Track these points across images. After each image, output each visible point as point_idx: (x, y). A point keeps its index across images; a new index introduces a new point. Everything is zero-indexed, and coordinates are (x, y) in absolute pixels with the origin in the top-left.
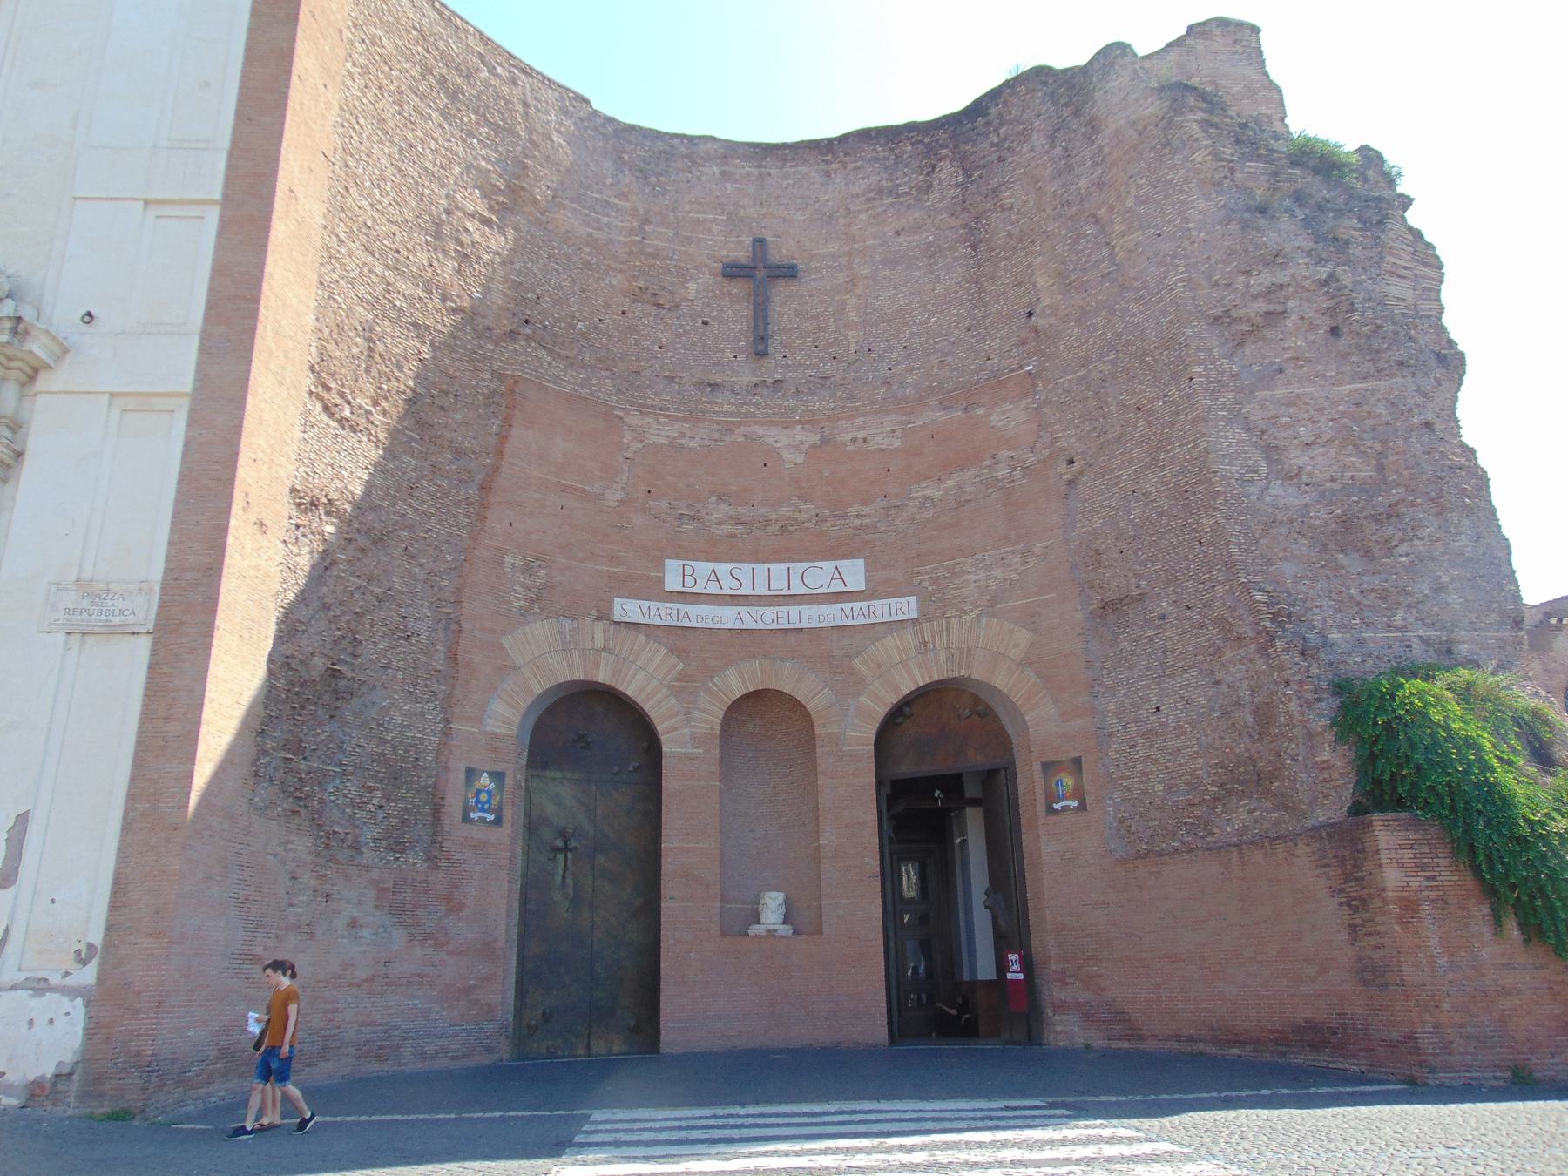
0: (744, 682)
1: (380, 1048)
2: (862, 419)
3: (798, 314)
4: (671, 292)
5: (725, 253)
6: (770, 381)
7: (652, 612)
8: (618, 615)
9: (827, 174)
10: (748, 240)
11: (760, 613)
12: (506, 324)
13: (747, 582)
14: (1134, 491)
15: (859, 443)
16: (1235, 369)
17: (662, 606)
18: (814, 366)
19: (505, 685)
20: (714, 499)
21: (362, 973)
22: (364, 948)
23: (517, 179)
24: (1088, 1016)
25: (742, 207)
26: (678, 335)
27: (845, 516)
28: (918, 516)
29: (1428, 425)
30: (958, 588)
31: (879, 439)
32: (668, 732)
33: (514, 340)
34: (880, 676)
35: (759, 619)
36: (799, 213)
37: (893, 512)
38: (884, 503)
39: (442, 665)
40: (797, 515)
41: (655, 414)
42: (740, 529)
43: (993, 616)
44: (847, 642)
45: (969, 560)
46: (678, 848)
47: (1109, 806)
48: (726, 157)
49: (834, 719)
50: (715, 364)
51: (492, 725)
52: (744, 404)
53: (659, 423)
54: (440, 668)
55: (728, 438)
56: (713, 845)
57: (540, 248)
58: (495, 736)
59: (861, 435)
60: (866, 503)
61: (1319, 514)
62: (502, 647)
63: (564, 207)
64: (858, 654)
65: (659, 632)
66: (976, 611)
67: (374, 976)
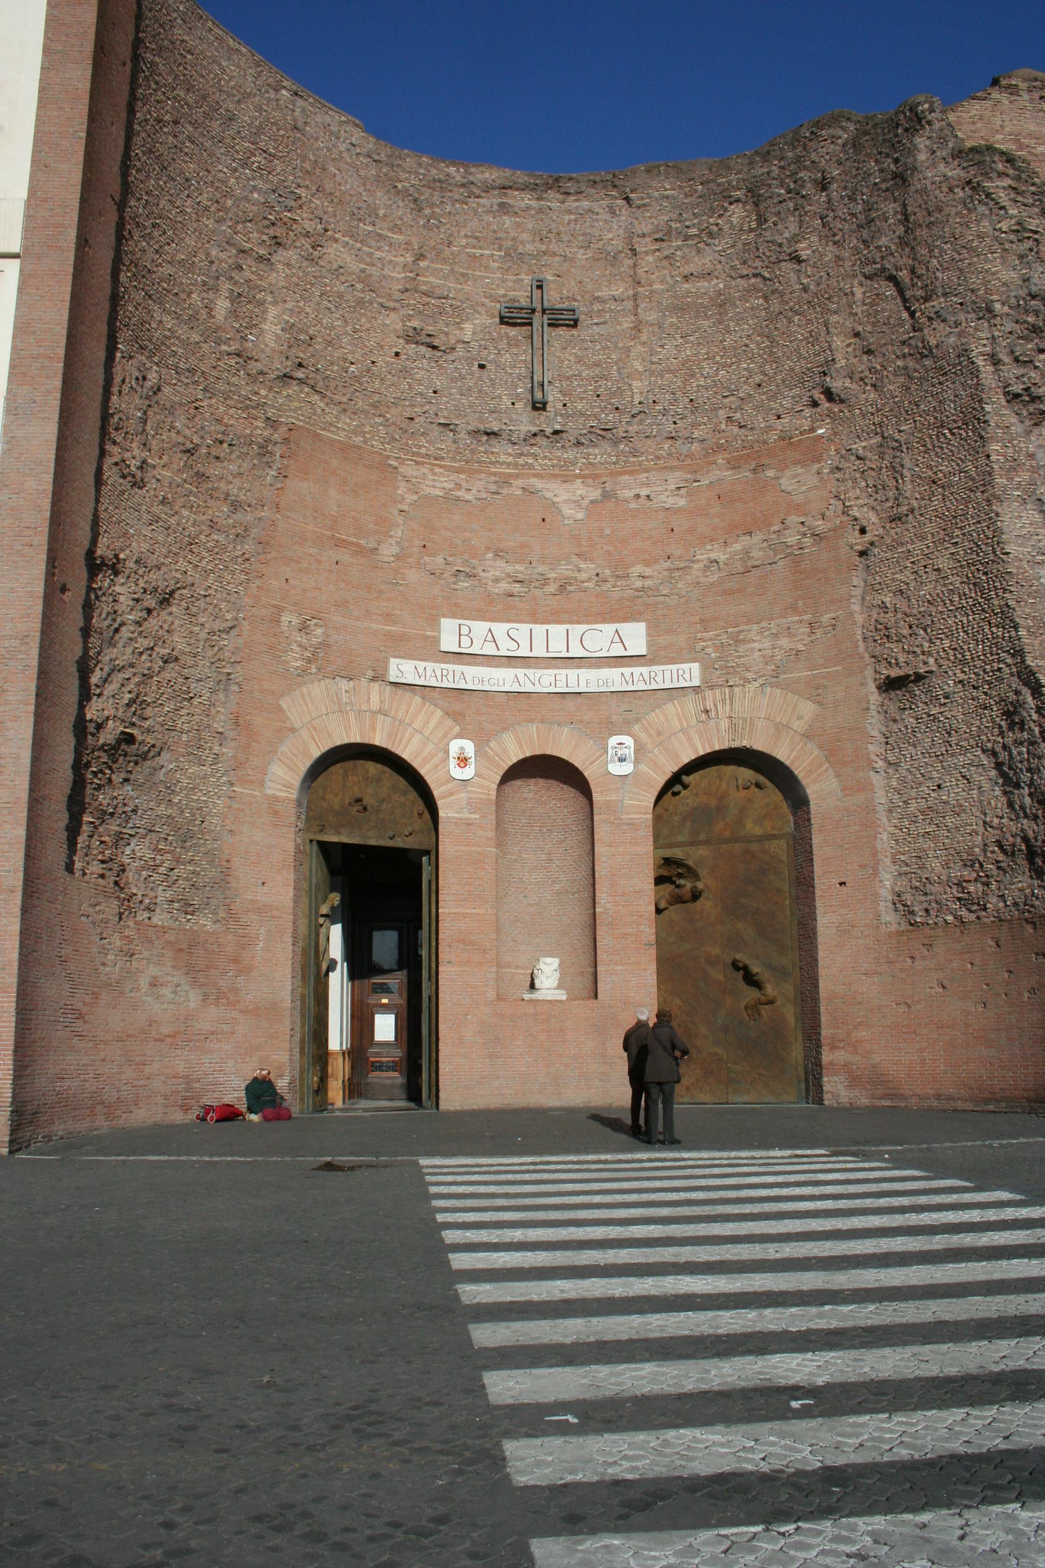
0: (521, 747)
1: (186, 1098)
2: (646, 475)
3: (579, 360)
4: (447, 334)
5: (502, 292)
6: (549, 431)
7: (428, 674)
8: (393, 676)
9: (612, 212)
10: (527, 279)
11: (538, 676)
12: (279, 366)
13: (525, 644)
14: (925, 567)
15: (642, 501)
16: (1031, 449)
17: (438, 667)
18: (596, 416)
19: (284, 748)
20: (490, 555)
21: (166, 1030)
22: (165, 1006)
23: (289, 211)
24: (854, 1081)
25: (521, 243)
26: (453, 380)
27: (627, 576)
28: (703, 580)
30: (741, 656)
31: (663, 498)
32: (444, 797)
33: (286, 385)
34: (660, 744)
35: (537, 683)
36: (582, 251)
37: (677, 574)
38: (668, 564)
39: (223, 727)
40: (577, 575)
41: (430, 464)
42: (517, 588)
43: (777, 685)
44: (627, 708)
45: (755, 627)
46: (456, 913)
47: (887, 880)
48: (504, 188)
49: (612, 786)
50: (492, 412)
51: (272, 789)
52: (521, 454)
53: (434, 474)
54: (220, 730)
55: (504, 491)
56: (490, 911)
57: (312, 285)
58: (275, 799)
59: (644, 492)
60: (648, 563)
62: (280, 709)
63: (336, 240)
64: (637, 720)
65: (435, 694)
66: (761, 681)
67: (175, 1033)
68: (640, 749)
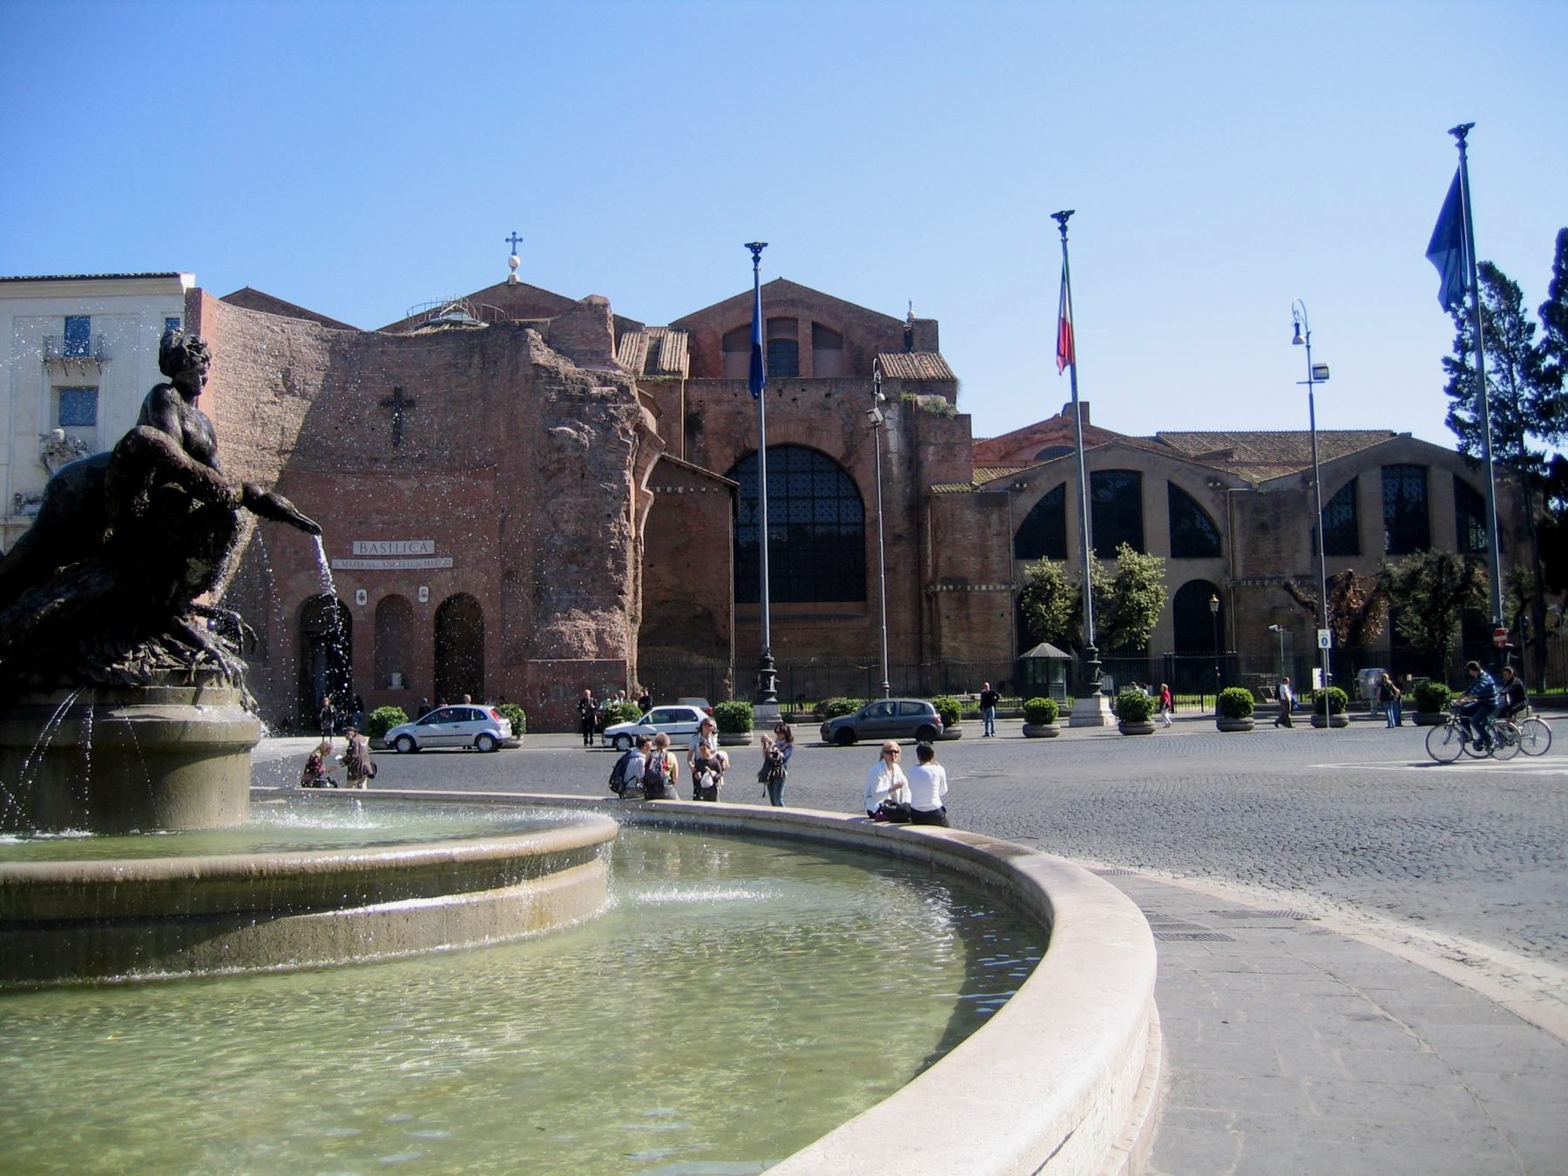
9: (429, 351)
17: (352, 562)
29: (609, 516)
61: (566, 548)
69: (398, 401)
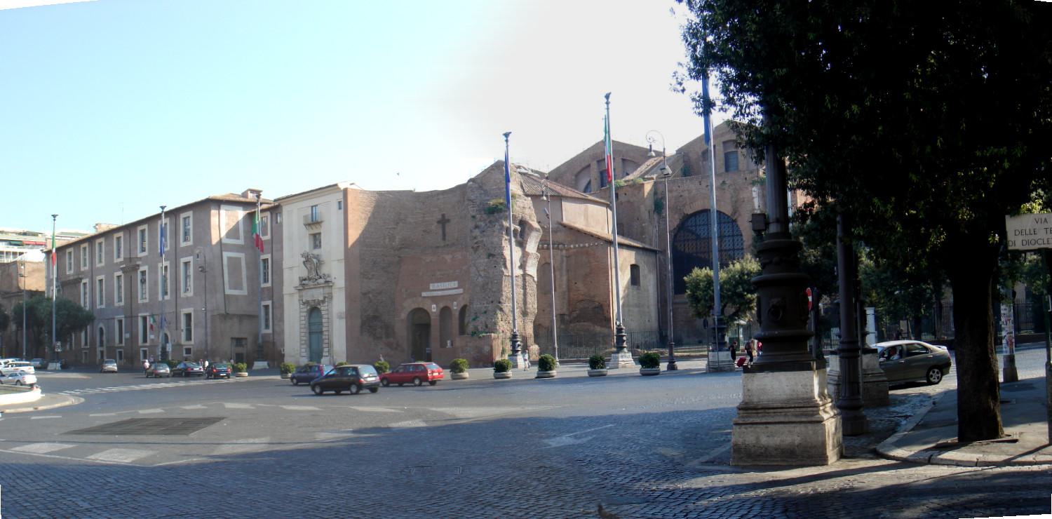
8: (423, 295)
68: (457, 304)
69: (443, 222)
